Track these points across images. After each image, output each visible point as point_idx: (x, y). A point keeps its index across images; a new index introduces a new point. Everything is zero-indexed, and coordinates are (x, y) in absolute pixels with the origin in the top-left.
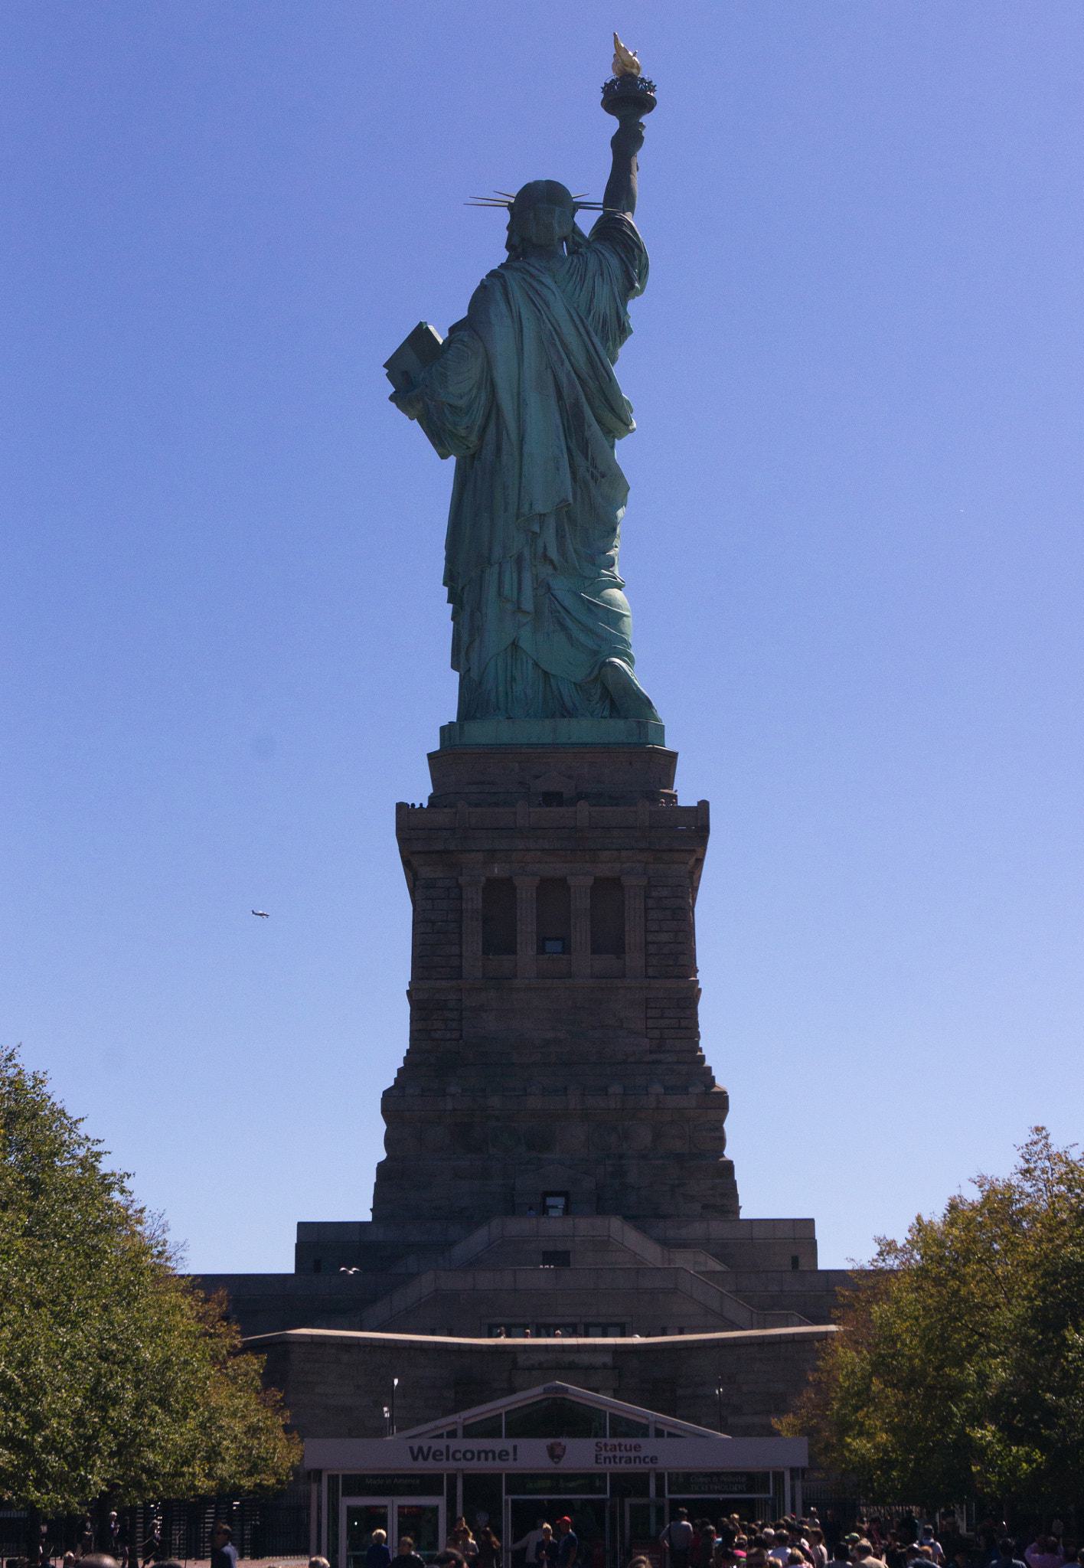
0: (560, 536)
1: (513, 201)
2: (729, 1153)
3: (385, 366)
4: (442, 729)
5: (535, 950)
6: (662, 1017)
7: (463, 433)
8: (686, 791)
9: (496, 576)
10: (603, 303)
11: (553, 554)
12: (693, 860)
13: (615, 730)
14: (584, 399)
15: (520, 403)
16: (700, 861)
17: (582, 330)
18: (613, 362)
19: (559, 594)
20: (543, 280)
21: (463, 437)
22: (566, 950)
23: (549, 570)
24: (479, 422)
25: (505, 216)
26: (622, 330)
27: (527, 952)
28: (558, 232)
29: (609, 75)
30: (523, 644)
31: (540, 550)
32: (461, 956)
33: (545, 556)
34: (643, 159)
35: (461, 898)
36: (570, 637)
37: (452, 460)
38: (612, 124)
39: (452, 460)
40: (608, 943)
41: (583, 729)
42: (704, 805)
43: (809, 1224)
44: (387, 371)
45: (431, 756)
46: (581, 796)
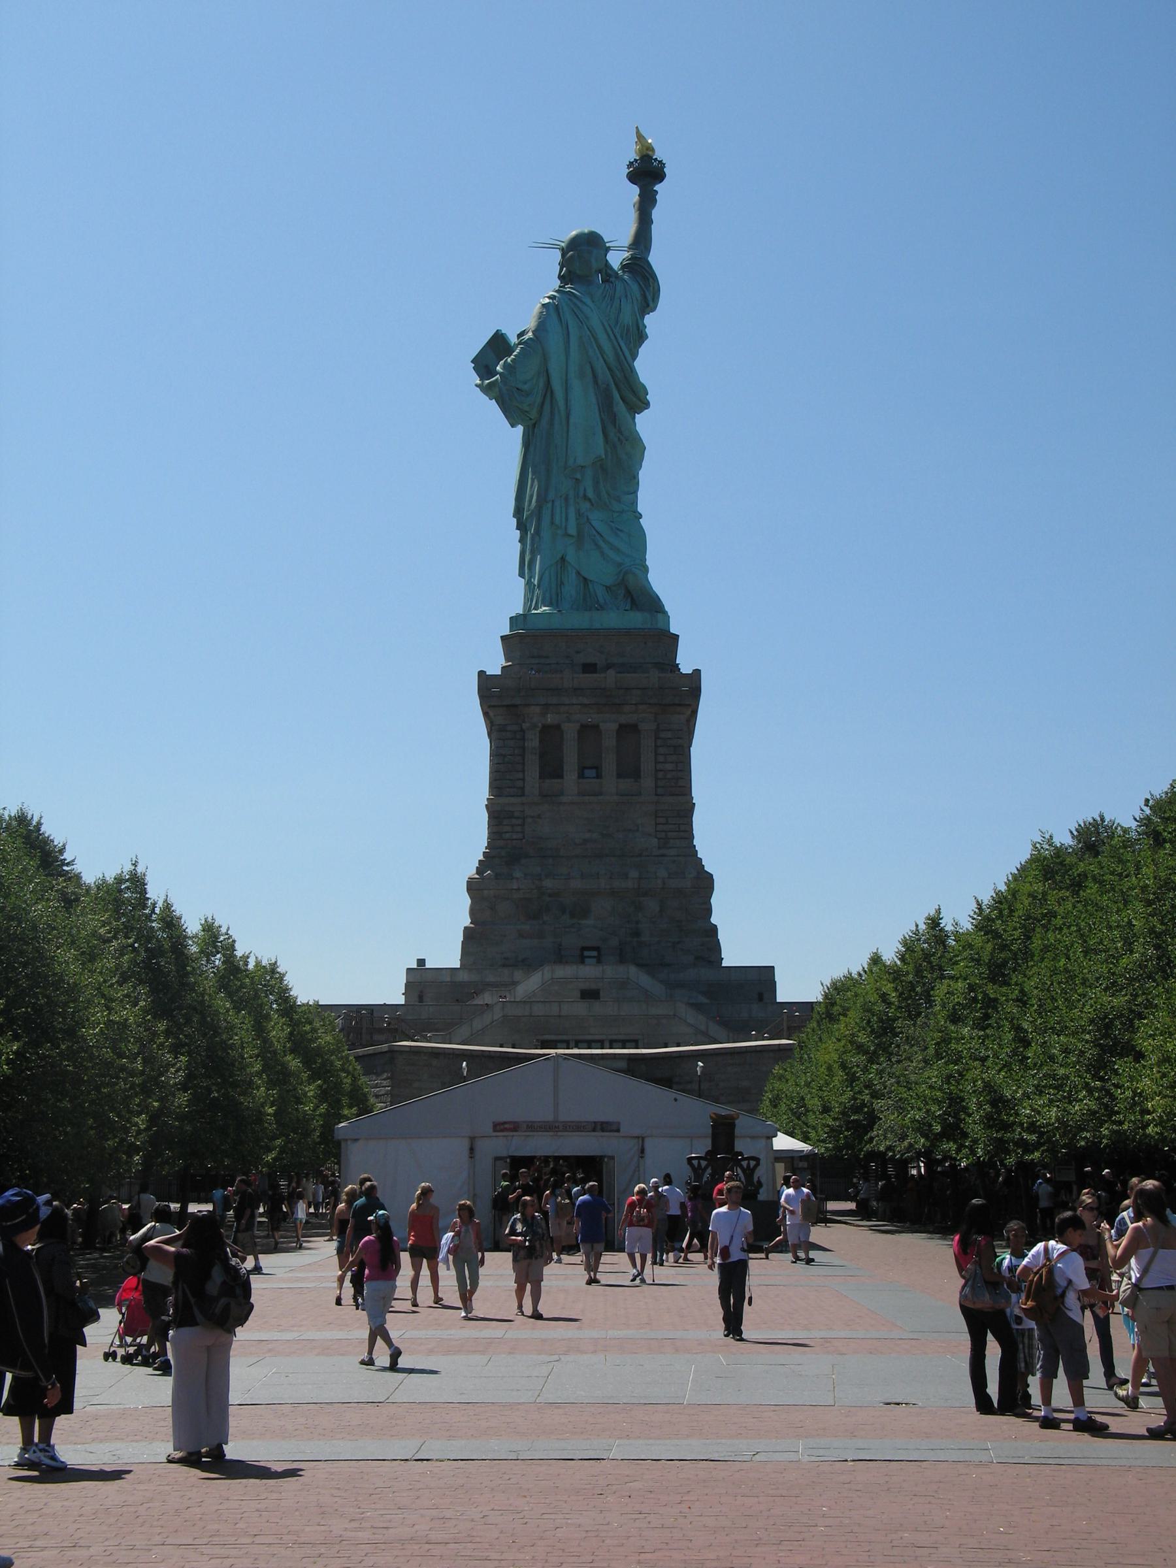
0: (596, 484)
1: (563, 244)
2: (714, 920)
3: (472, 362)
4: (511, 618)
5: (577, 775)
6: (666, 823)
7: (527, 409)
8: (686, 663)
10: (627, 318)
11: (590, 494)
12: (689, 712)
13: (636, 619)
14: (613, 386)
15: (567, 389)
16: (694, 713)
17: (612, 337)
18: (634, 359)
19: (594, 523)
20: (584, 300)
21: (526, 412)
22: (599, 776)
23: (588, 505)
24: (539, 400)
25: (557, 256)
26: (641, 336)
28: (595, 265)
29: (633, 155)
30: (568, 558)
31: (581, 493)
32: (523, 780)
33: (585, 497)
34: (656, 214)
35: (523, 739)
36: (602, 553)
38: (635, 190)
40: (630, 771)
41: (613, 619)
42: (697, 672)
43: (771, 969)
44: (473, 365)
45: (503, 638)
46: (609, 667)
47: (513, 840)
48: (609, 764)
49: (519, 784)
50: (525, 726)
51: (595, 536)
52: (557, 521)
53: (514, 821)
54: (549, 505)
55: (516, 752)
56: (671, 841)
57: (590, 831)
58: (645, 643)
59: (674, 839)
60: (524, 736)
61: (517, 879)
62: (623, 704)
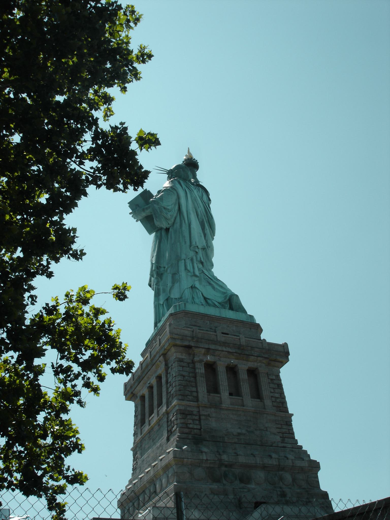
9: (183, 264)
24: (175, 215)
27: (225, 394)
32: (197, 392)
37: (154, 234)
39: (154, 234)
47: (194, 429)
48: (246, 388)
49: (195, 394)
50: (196, 359)
51: (208, 279)
52: (189, 268)
53: (194, 417)
54: (183, 261)
55: (190, 375)
56: (286, 439)
57: (240, 428)
58: (250, 329)
59: (288, 438)
60: (194, 366)
61: (205, 453)
62: (250, 355)
